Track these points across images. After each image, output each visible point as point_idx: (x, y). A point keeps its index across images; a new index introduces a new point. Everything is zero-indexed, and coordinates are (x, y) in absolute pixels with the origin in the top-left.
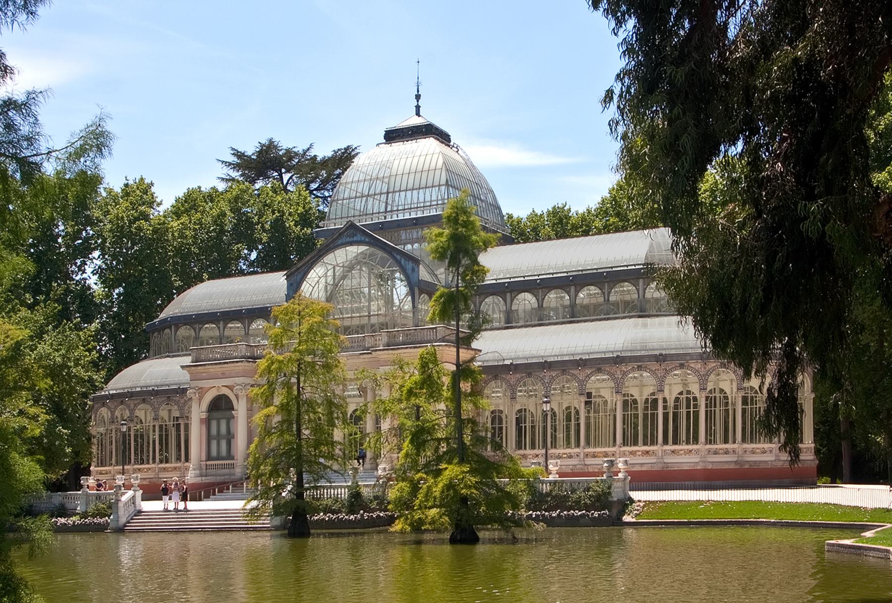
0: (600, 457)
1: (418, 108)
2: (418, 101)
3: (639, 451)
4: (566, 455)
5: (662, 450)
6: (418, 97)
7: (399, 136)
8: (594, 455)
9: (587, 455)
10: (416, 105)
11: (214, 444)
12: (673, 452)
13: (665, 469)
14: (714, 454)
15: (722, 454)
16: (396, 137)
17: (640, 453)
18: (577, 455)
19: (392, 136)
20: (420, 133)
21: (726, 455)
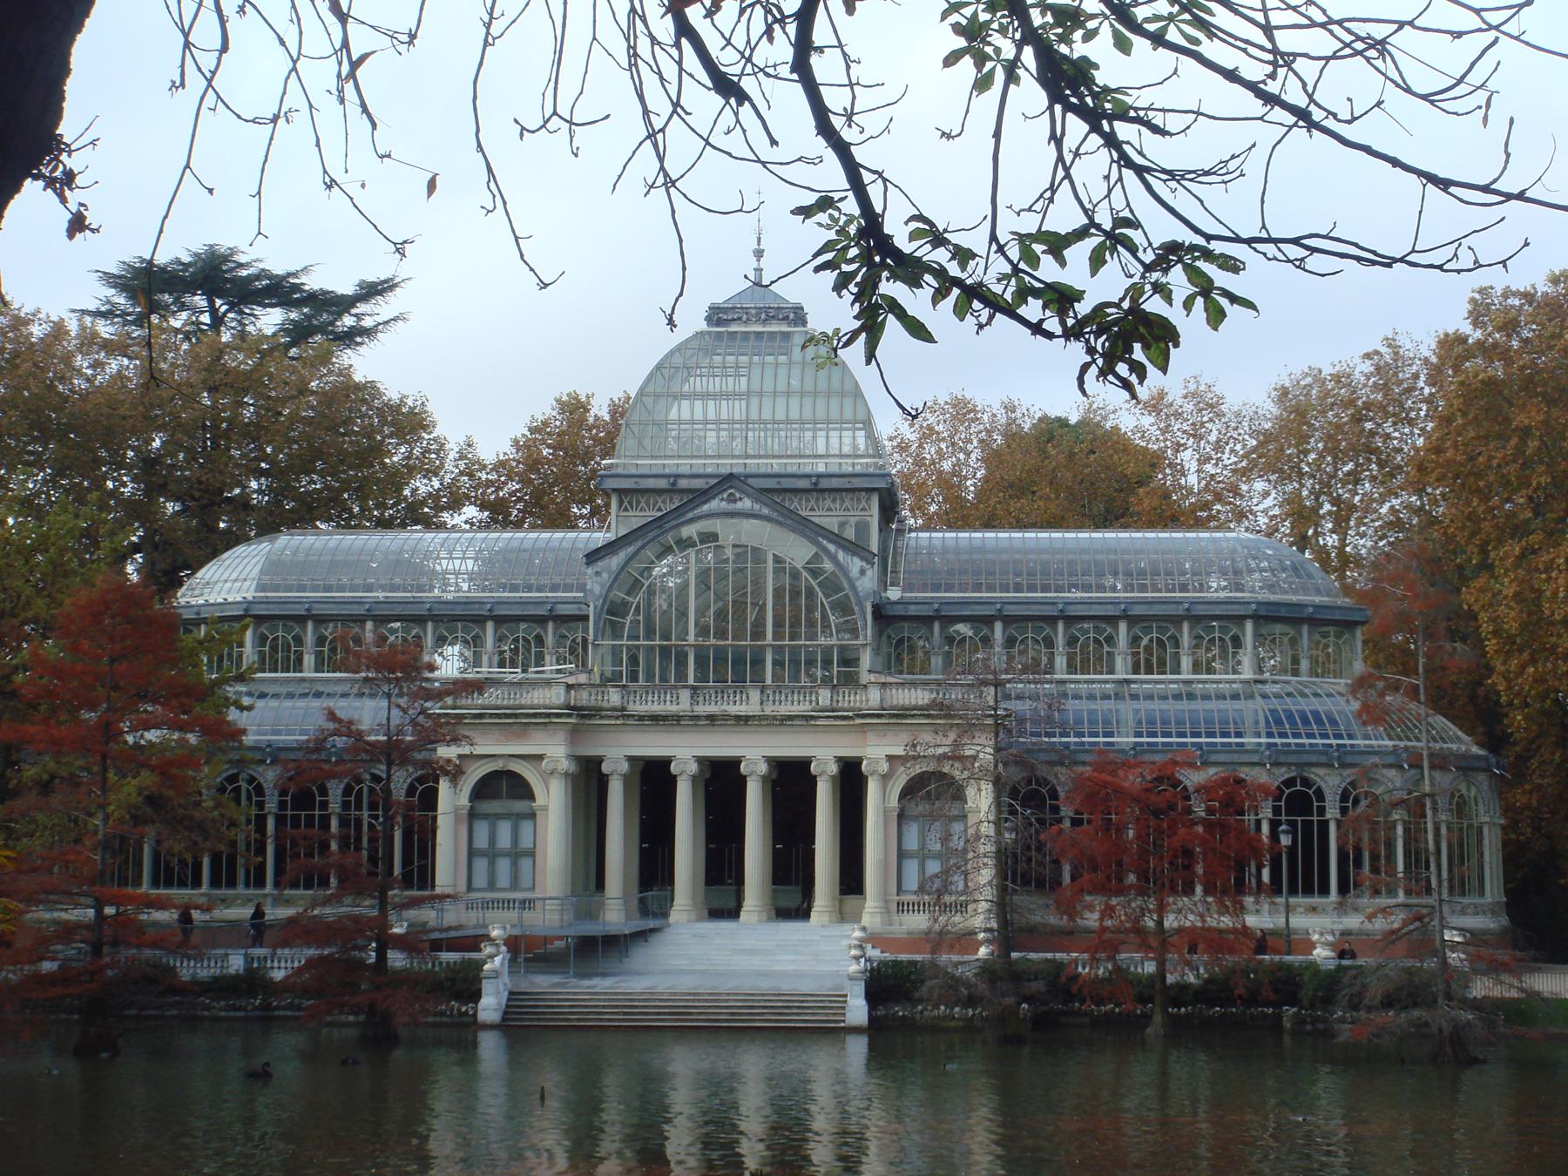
6: (759, 254)
7: (740, 319)
10: (755, 265)
11: (481, 865)
16: (734, 320)
17: (1302, 910)
20: (783, 319)
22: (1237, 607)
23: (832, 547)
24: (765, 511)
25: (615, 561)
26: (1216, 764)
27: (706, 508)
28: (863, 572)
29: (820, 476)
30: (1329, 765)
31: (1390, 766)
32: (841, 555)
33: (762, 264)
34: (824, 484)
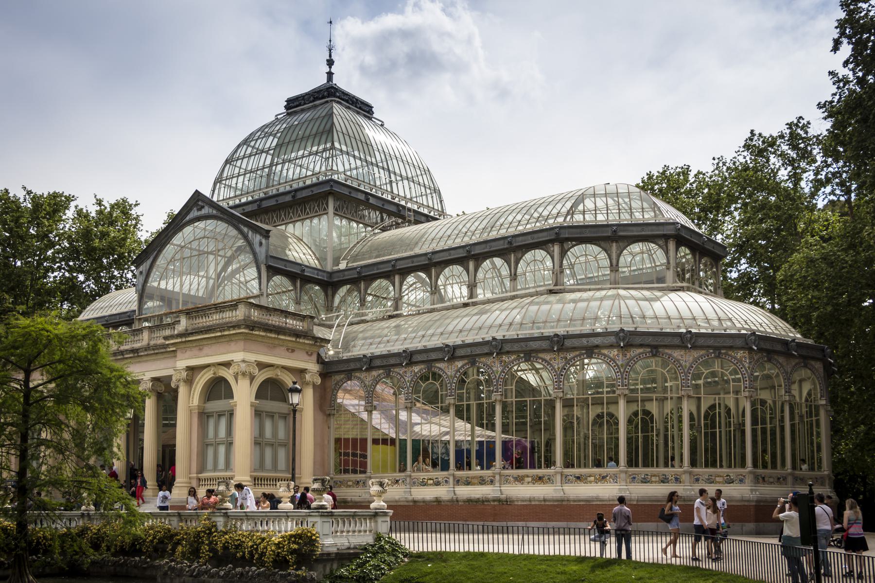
0: (474, 484)
1: (330, 75)
2: (330, 67)
3: (528, 476)
4: (431, 482)
5: (562, 475)
6: (330, 63)
8: (467, 481)
9: (458, 481)
10: (328, 70)
12: (578, 478)
13: (564, 503)
14: (642, 482)
15: (655, 482)
17: (530, 479)
18: (446, 481)
19: (294, 104)
21: (662, 484)
22: (545, 234)
23: (245, 230)
24: (214, 212)
25: (149, 262)
26: (462, 358)
27: (188, 218)
28: (261, 244)
29: (296, 190)
30: (551, 350)
31: (611, 346)
32: (250, 233)
33: (333, 70)
34: (300, 195)
